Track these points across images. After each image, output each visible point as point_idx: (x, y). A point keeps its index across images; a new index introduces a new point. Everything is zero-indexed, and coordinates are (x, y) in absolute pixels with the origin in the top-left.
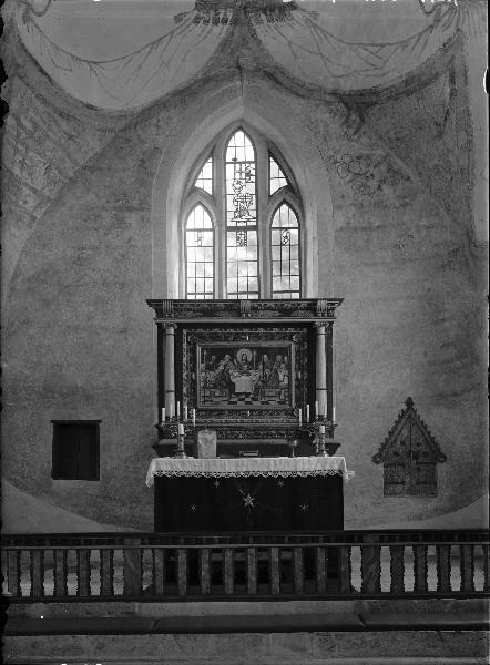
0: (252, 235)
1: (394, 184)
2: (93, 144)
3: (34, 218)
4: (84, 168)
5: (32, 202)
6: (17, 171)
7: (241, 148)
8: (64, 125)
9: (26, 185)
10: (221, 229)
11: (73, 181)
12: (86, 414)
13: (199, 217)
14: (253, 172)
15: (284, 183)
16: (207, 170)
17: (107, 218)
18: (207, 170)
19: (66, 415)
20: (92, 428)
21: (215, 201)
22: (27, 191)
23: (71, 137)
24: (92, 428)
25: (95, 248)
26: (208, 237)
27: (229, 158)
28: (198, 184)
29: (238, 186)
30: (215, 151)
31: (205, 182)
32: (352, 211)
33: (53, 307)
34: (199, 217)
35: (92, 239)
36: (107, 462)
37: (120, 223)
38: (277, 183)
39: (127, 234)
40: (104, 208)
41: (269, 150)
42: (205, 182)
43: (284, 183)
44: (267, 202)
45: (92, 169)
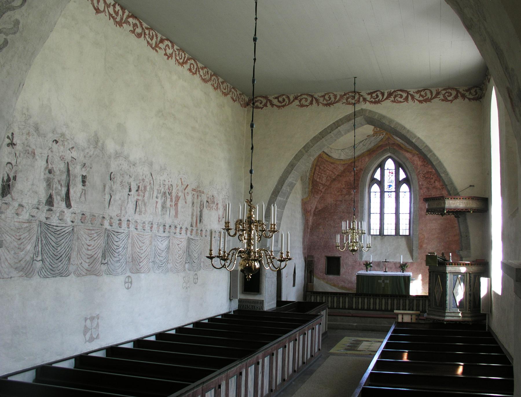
0: (394, 194)
1: (439, 181)
2: (341, 168)
3: (321, 192)
4: (338, 175)
5: (321, 187)
6: (318, 180)
7: (390, 164)
8: (333, 166)
9: (320, 183)
10: (382, 193)
11: (334, 180)
12: (337, 255)
13: (375, 188)
14: (394, 173)
15: (404, 176)
16: (379, 171)
17: (345, 191)
18: (379, 171)
19: (330, 255)
20: (338, 259)
21: (381, 184)
22: (320, 185)
23: (334, 168)
24: (338, 259)
25: (341, 201)
26: (378, 194)
27: (386, 168)
28: (375, 177)
29: (389, 179)
30: (382, 166)
31: (377, 176)
32: (425, 190)
33: (327, 220)
34: (375, 188)
35: (340, 199)
36: (342, 270)
37: (349, 193)
38: (402, 175)
39: (351, 196)
40: (344, 188)
41: (398, 165)
42: (377, 176)
43: (404, 176)
44: (398, 184)
45: (341, 176)
